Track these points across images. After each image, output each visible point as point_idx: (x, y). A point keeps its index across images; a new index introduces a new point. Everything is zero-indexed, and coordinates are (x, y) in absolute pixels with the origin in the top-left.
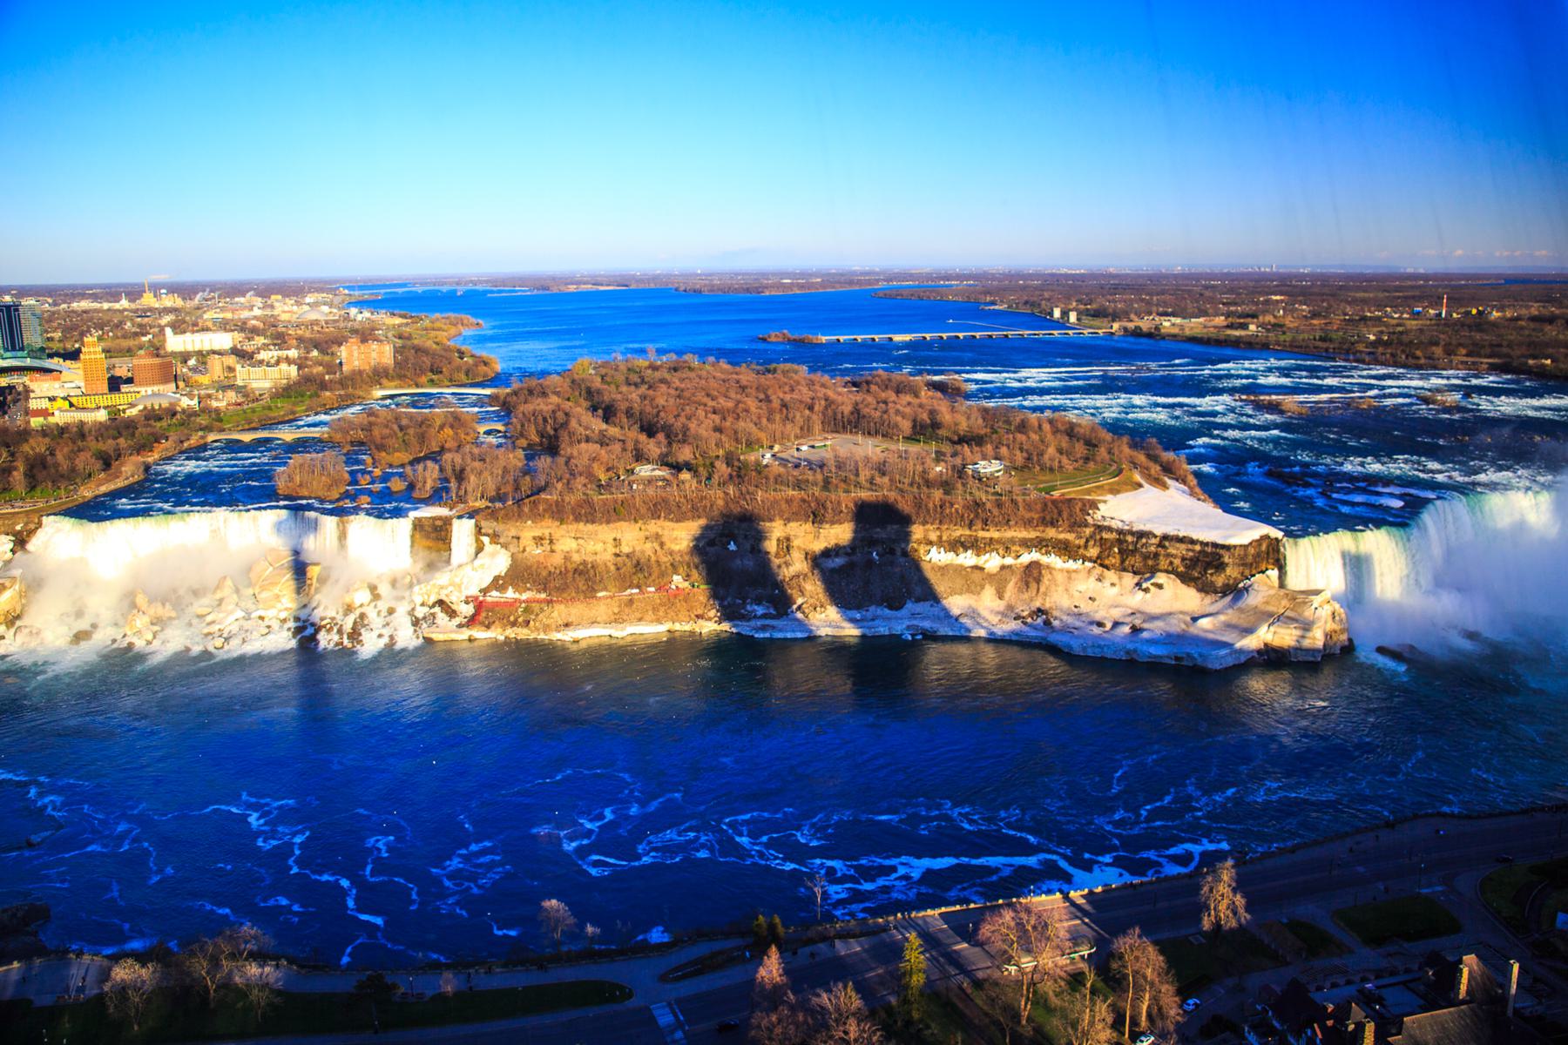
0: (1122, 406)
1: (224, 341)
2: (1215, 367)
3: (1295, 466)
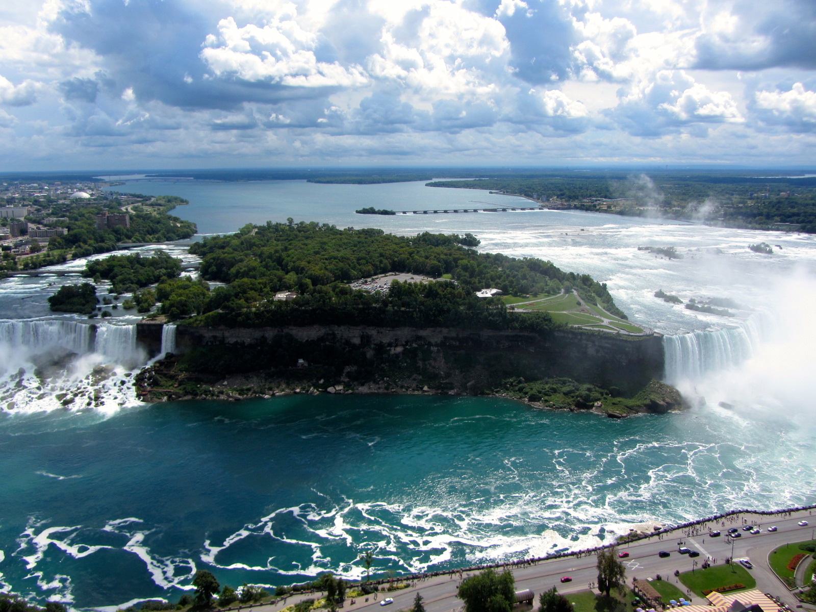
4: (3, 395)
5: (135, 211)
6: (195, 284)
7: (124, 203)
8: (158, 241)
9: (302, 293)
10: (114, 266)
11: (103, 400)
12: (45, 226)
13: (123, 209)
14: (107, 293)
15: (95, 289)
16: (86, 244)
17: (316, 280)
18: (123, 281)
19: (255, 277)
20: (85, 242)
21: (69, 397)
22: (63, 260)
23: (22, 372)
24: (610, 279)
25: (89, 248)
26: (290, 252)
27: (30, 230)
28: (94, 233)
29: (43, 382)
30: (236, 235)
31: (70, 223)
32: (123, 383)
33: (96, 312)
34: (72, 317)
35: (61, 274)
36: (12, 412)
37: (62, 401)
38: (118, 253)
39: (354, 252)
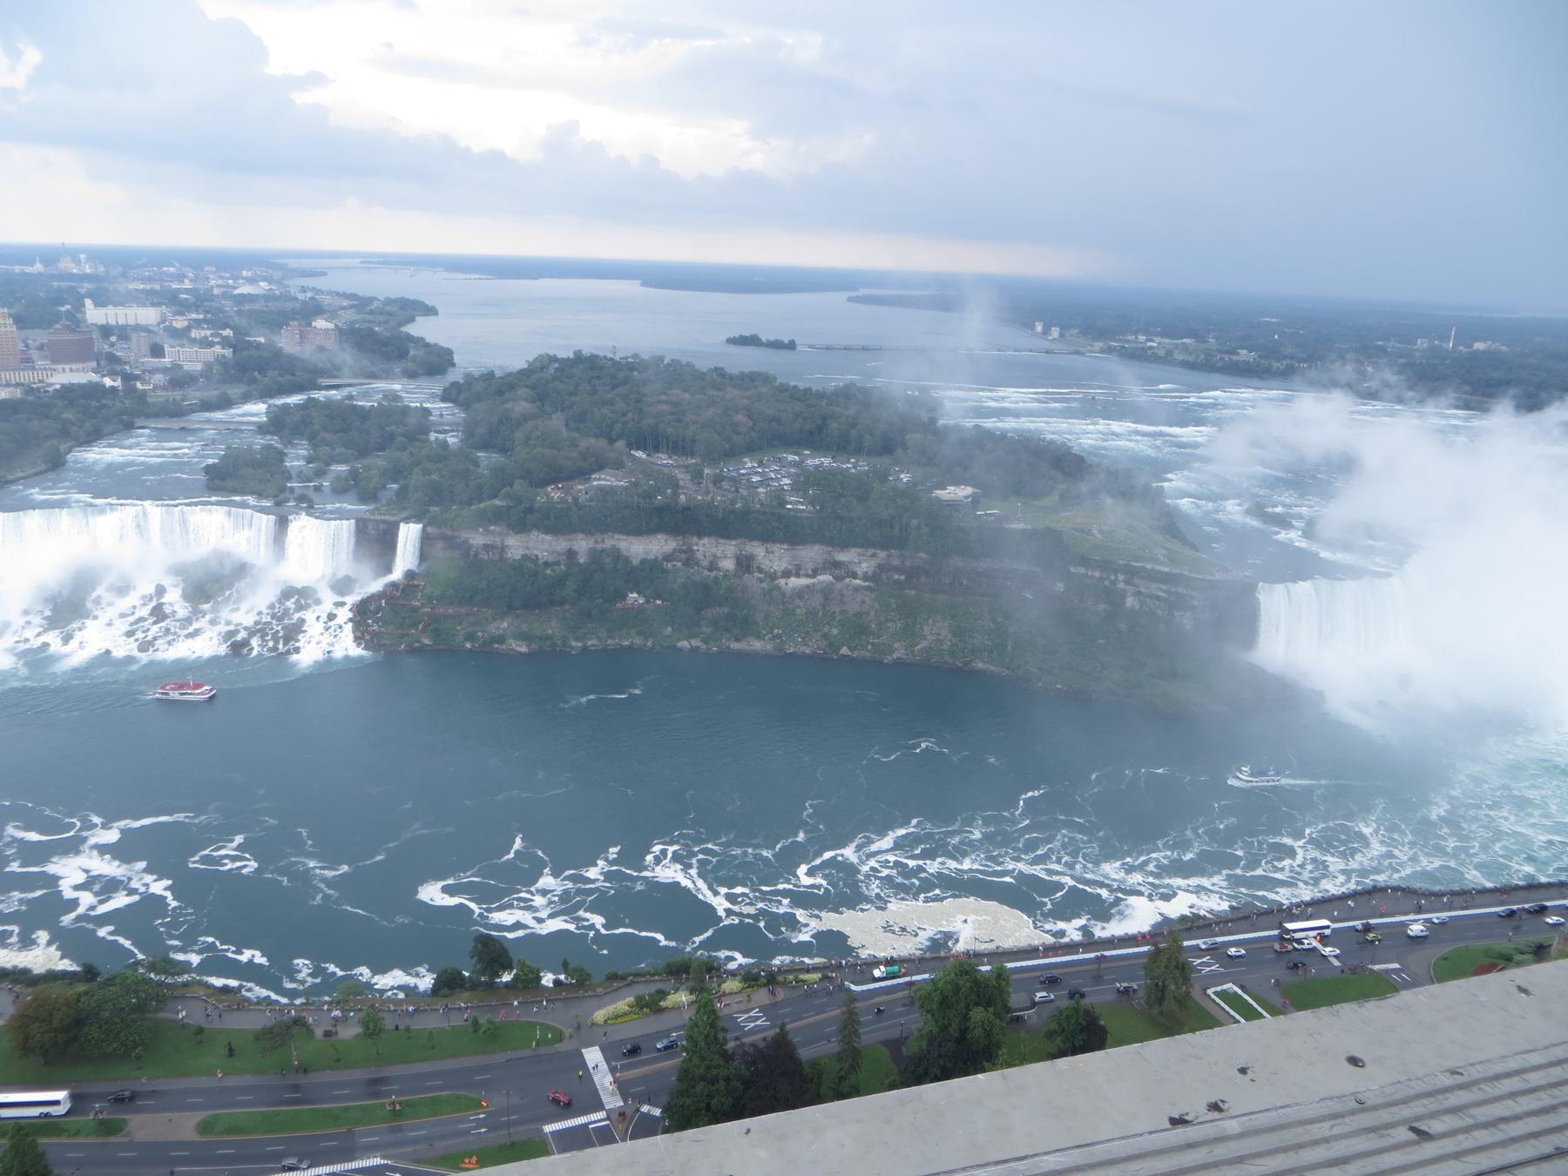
0: (1100, 433)
1: (148, 315)
2: (1201, 394)
3: (1277, 507)
4: (130, 628)
11: (297, 645)
14: (302, 463)
15: (286, 455)
22: (225, 403)
23: (161, 591)
24: (1170, 480)
29: (196, 613)
32: (331, 617)
33: (287, 494)
34: (244, 501)
36: (144, 658)
37: (229, 644)
38: (319, 395)
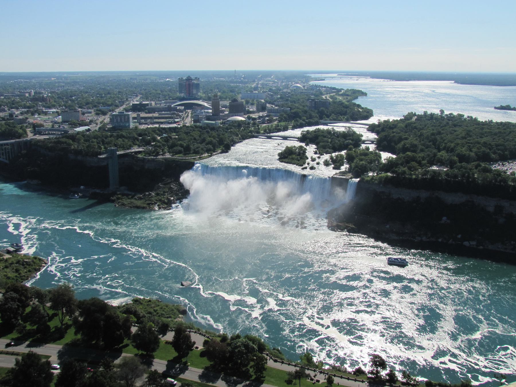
5: (331, 99)
6: (371, 153)
7: (324, 93)
8: (347, 121)
9: (451, 168)
10: (319, 136)
12: (276, 106)
13: (324, 97)
16: (301, 119)
17: (462, 158)
18: (324, 147)
19: (414, 151)
20: (300, 118)
21: (286, 220)
22: (285, 129)
25: (304, 122)
26: (442, 136)
27: (267, 108)
28: (305, 112)
30: (401, 120)
31: (292, 105)
33: (306, 165)
35: (285, 138)
38: (321, 127)
39: (494, 139)
